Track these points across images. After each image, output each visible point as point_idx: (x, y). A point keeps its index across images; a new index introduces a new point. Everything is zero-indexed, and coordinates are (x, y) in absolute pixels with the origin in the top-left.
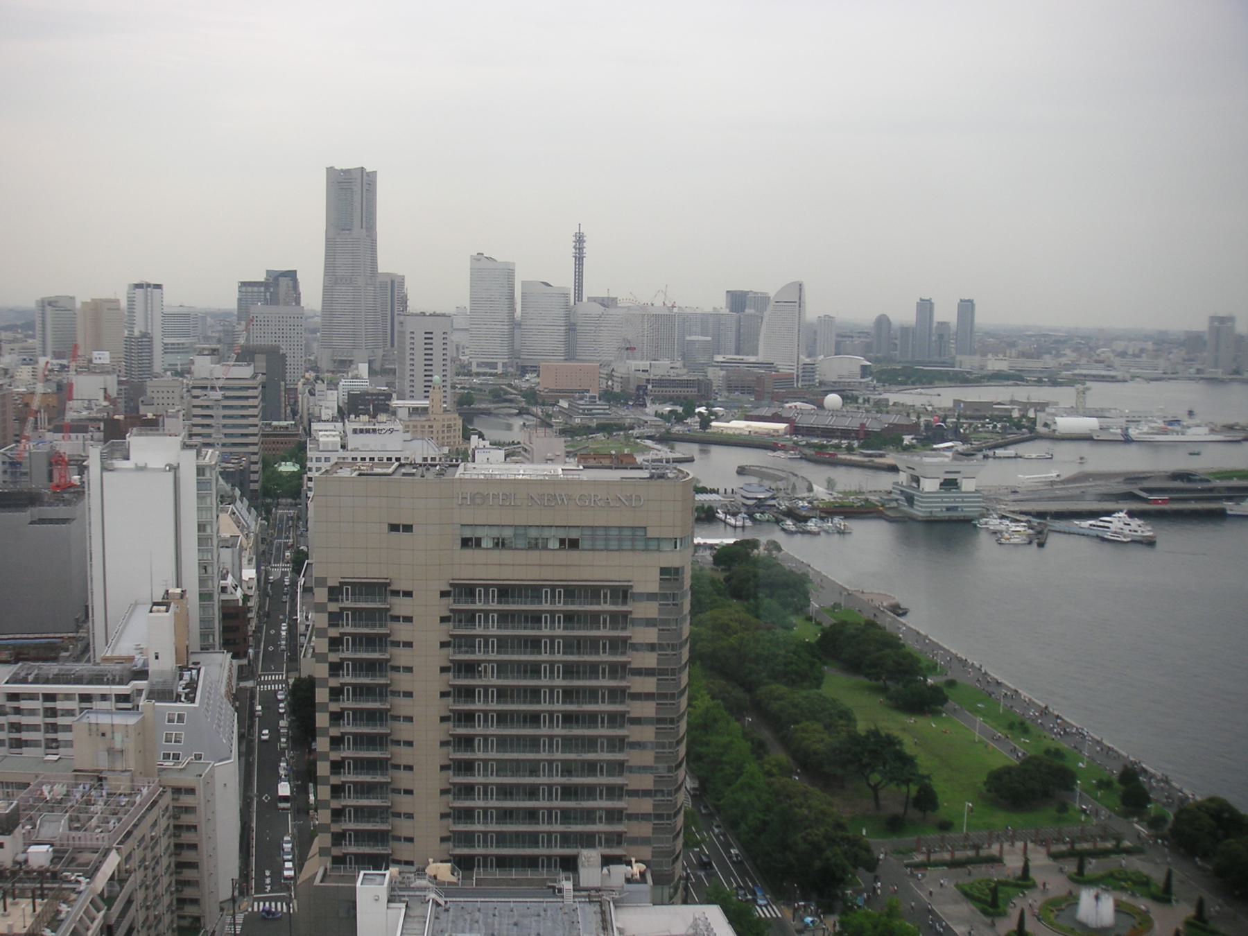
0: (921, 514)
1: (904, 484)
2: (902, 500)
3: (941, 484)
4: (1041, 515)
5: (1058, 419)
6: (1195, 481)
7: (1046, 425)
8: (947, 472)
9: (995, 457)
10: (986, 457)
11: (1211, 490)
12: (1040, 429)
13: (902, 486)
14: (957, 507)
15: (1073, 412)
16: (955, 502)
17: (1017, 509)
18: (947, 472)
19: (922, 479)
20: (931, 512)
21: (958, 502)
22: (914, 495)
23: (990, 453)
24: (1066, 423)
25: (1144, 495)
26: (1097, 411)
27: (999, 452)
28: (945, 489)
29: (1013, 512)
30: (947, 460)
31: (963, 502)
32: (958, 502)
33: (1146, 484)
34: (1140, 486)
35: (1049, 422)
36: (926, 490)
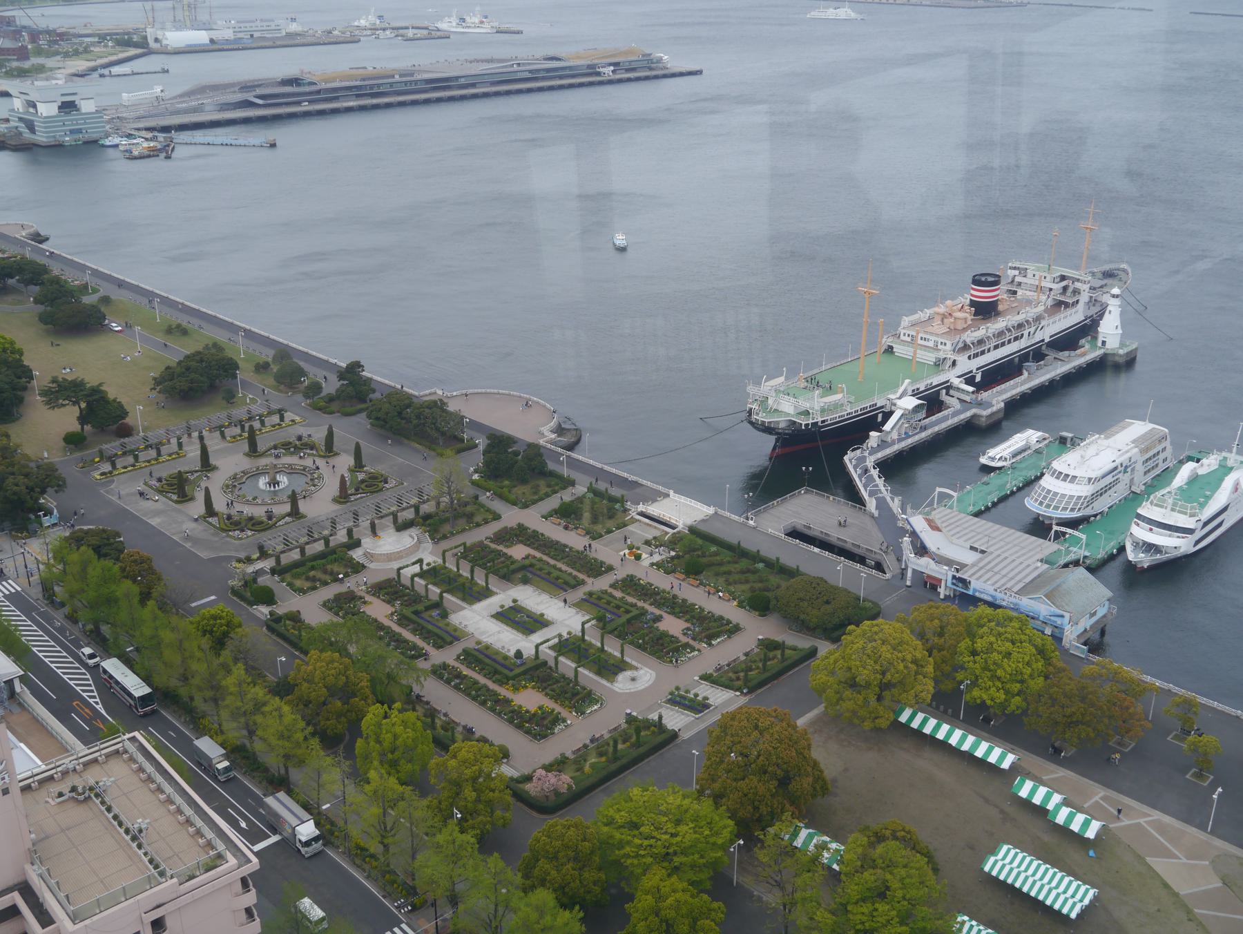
0: (44, 140)
1: (21, 110)
2: (22, 127)
3: (60, 108)
4: (166, 129)
5: (168, 34)
6: (304, 85)
7: (157, 40)
8: (63, 95)
9: (111, 75)
10: (102, 76)
11: (319, 92)
12: (152, 44)
13: (18, 112)
14: (81, 129)
15: (179, 25)
16: (77, 124)
17: (141, 125)
18: (63, 95)
19: (37, 103)
20: (54, 137)
21: (81, 124)
22: (33, 121)
23: (106, 72)
24: (175, 38)
25: (260, 102)
26: (204, 24)
27: (116, 70)
28: (66, 113)
29: (138, 129)
30: (60, 82)
31: (85, 123)
32: (81, 124)
33: (259, 91)
34: (254, 93)
35: (160, 37)
36: (44, 115)
